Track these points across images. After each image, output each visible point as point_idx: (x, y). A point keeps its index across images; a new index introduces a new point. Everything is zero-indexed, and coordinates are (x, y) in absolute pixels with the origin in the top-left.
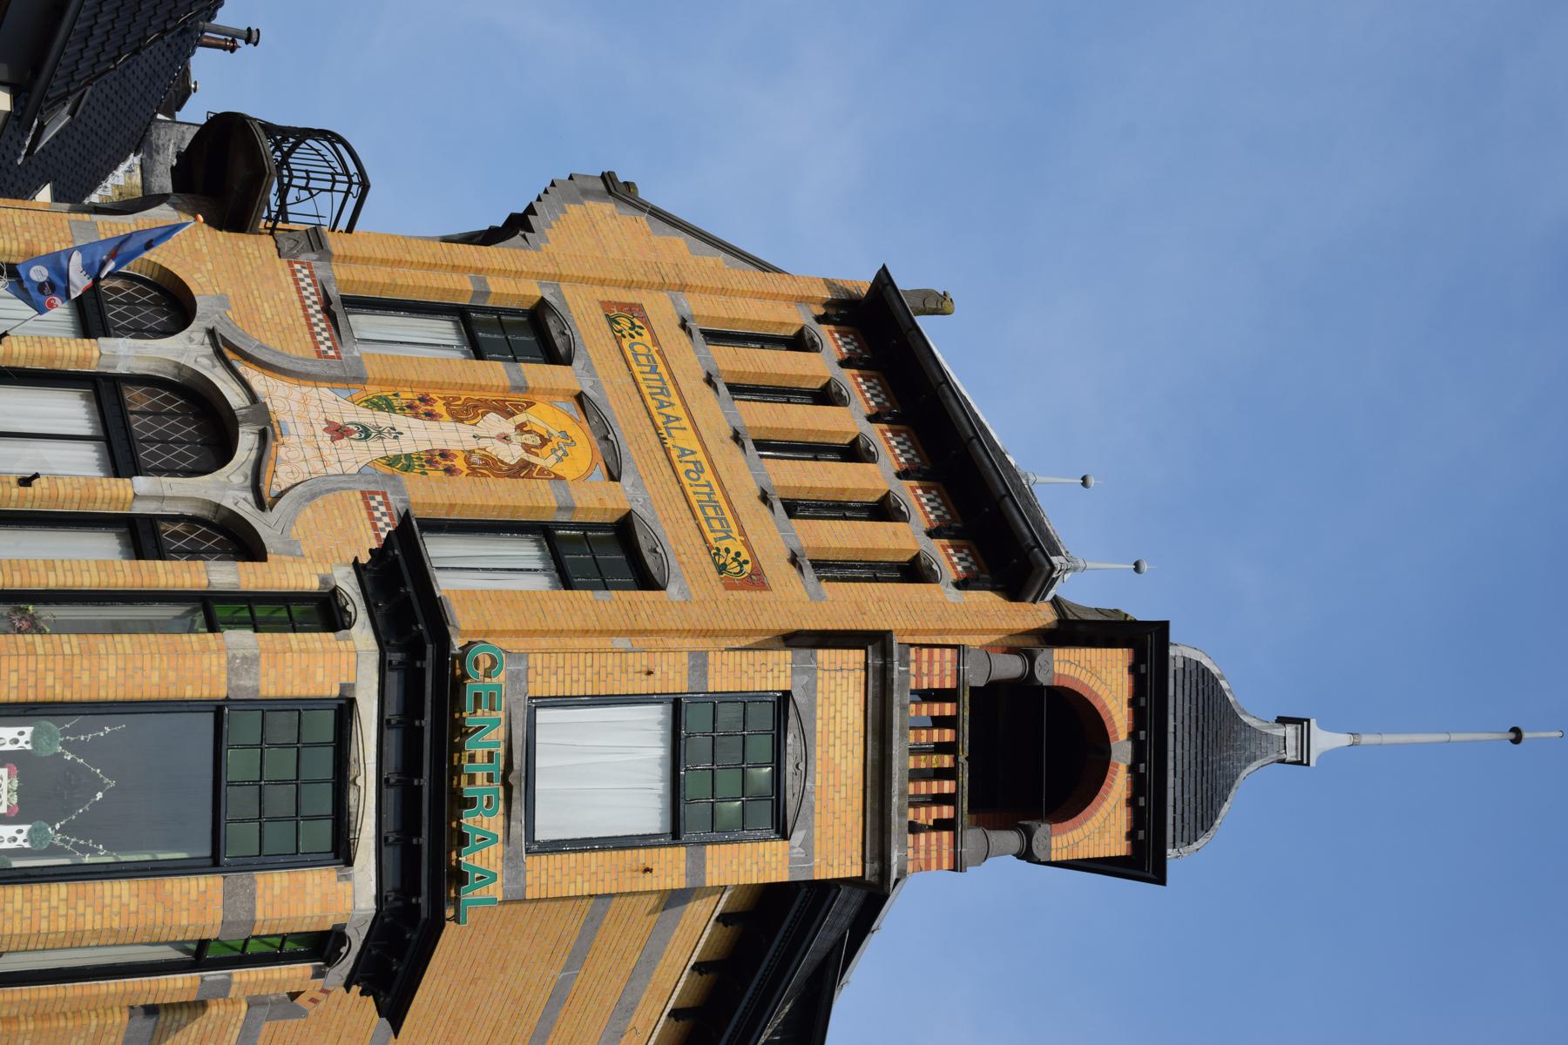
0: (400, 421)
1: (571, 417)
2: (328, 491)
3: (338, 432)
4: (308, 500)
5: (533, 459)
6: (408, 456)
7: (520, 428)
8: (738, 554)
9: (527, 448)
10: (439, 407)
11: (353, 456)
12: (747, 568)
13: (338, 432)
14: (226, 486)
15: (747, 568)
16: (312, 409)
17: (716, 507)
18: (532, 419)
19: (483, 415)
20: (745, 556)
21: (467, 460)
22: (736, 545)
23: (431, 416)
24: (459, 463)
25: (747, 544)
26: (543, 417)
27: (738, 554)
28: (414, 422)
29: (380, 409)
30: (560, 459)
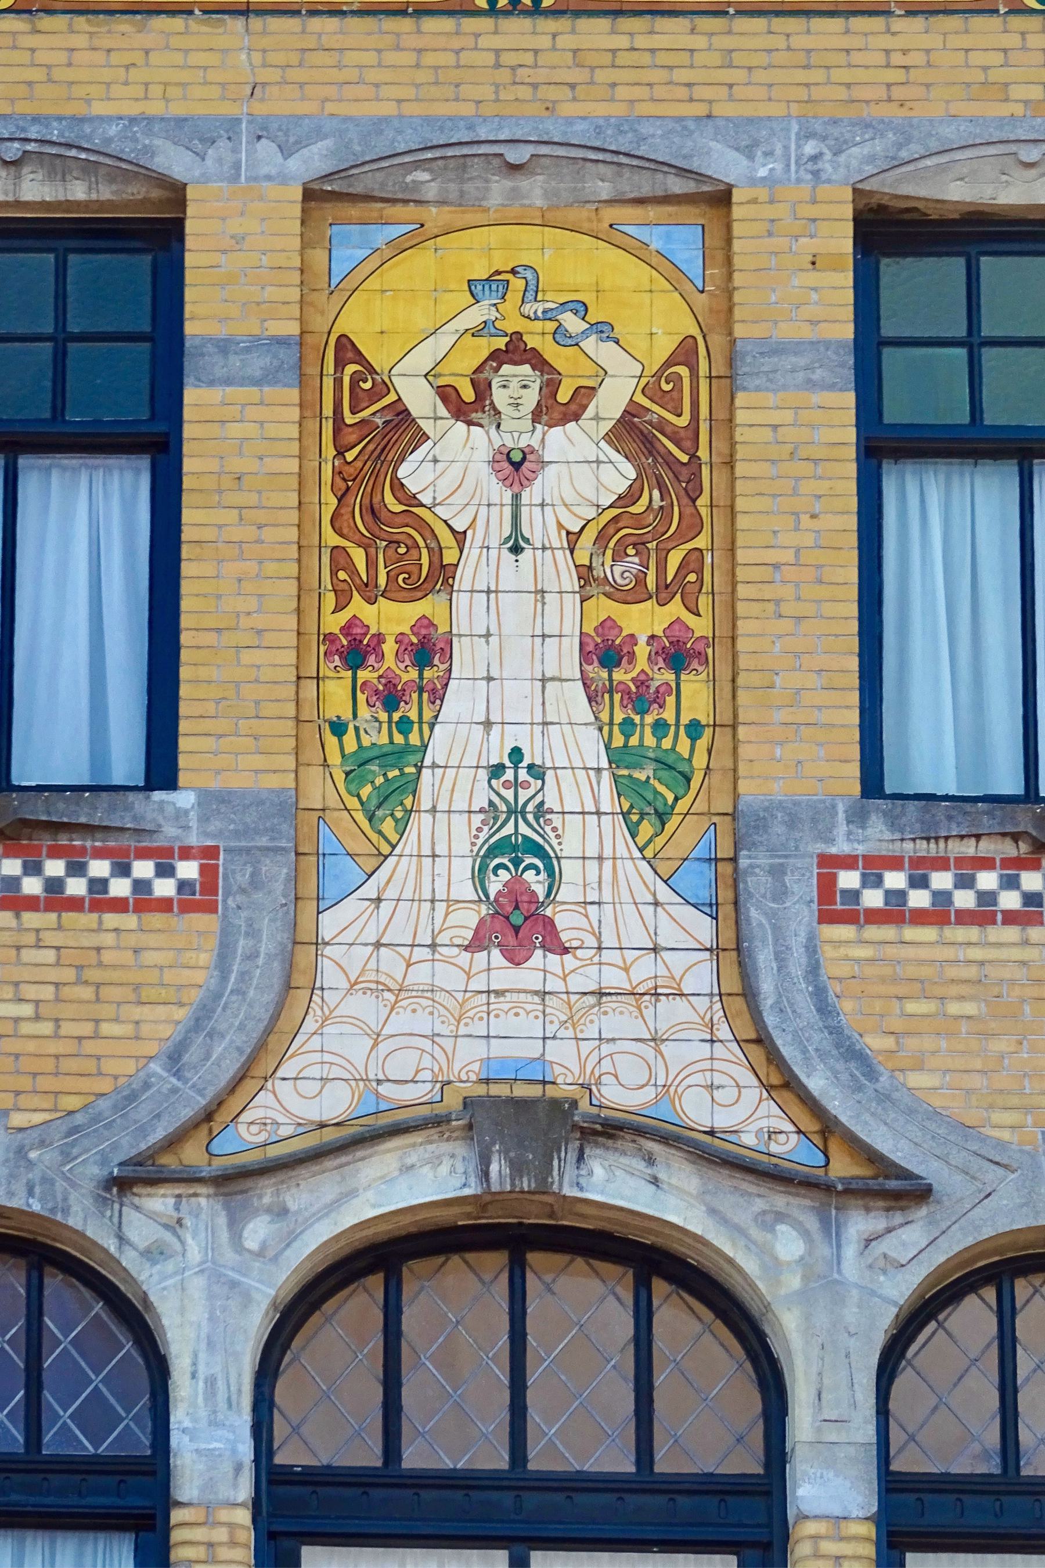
0: (457, 742)
1: (399, 248)
2: (824, 1008)
3: (519, 925)
4: (871, 1074)
5: (611, 402)
6: (617, 757)
7: (468, 405)
9: (557, 409)
10: (391, 619)
13: (519, 925)
14: (823, 1283)
16: (420, 975)
18: (423, 358)
19: (411, 500)
21: (633, 594)
23: (427, 648)
24: (644, 622)
26: (415, 327)
28: (461, 702)
29: (412, 785)
30: (603, 330)
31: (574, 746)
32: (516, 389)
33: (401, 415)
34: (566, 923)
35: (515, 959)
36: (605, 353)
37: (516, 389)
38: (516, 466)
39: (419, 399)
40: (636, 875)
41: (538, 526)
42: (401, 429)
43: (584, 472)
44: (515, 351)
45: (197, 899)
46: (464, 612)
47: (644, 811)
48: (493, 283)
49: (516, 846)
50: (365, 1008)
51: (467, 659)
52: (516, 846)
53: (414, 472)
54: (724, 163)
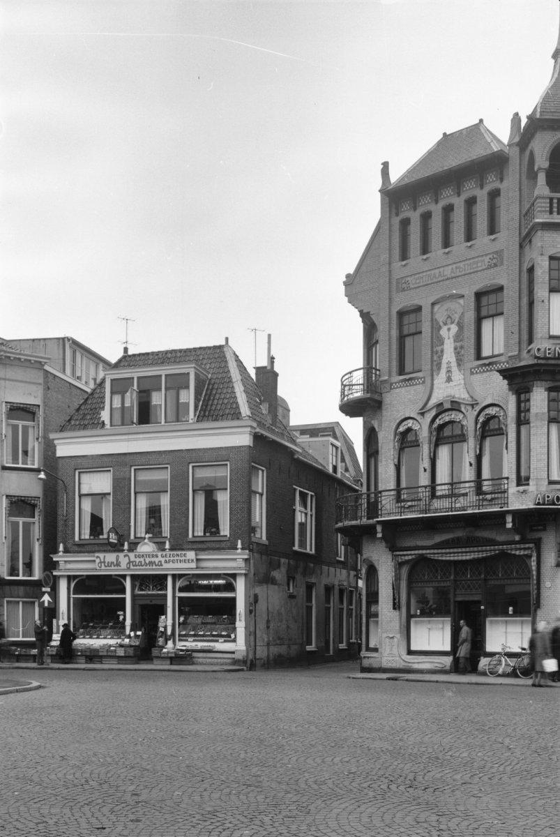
0: (444, 361)
3: (449, 380)
5: (456, 321)
7: (445, 324)
8: (490, 259)
9: (452, 323)
11: (457, 376)
12: (495, 256)
13: (449, 380)
15: (495, 256)
17: (474, 263)
20: (491, 256)
22: (487, 259)
24: (458, 344)
25: (486, 255)
27: (490, 259)
28: (445, 357)
30: (456, 313)
31: (453, 360)
32: (449, 321)
33: (440, 326)
34: (452, 378)
35: (449, 383)
36: (456, 315)
37: (449, 321)
38: (449, 329)
39: (441, 324)
40: (458, 372)
41: (451, 336)
42: (440, 328)
43: (454, 328)
44: (449, 317)
45: (424, 382)
46: (445, 347)
47: (459, 365)
48: (447, 310)
49: (449, 371)
50: (437, 390)
51: (445, 351)
52: (449, 371)
53: (441, 332)
54: (463, 293)
